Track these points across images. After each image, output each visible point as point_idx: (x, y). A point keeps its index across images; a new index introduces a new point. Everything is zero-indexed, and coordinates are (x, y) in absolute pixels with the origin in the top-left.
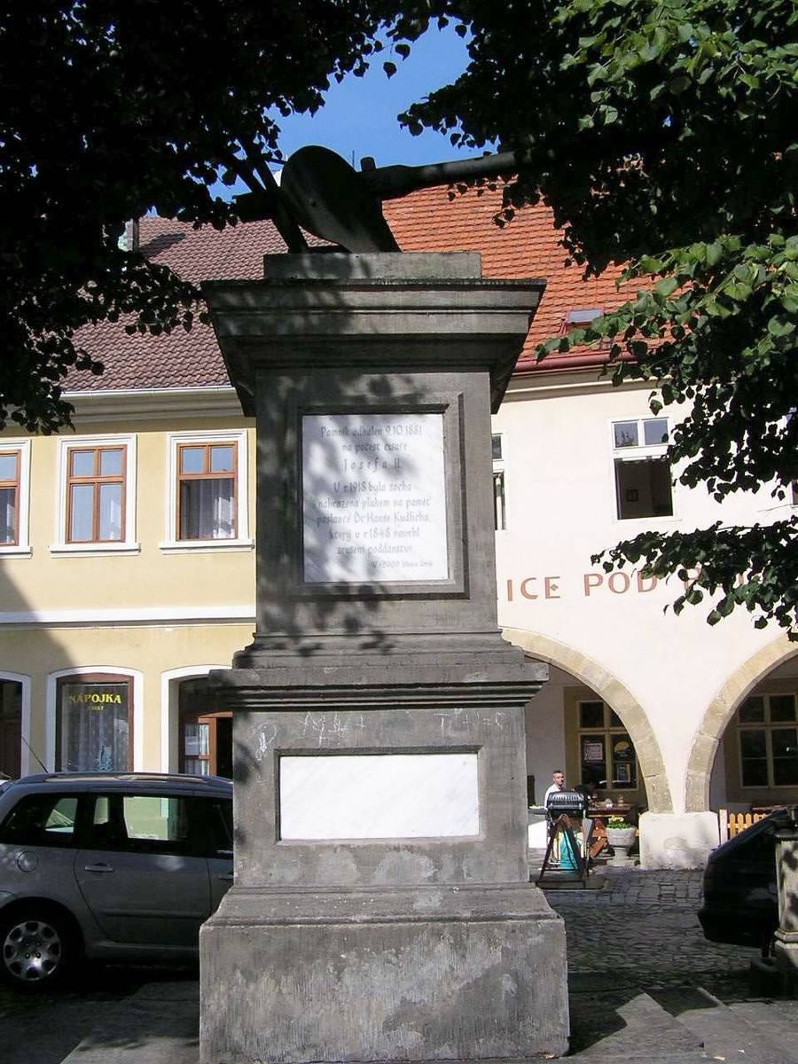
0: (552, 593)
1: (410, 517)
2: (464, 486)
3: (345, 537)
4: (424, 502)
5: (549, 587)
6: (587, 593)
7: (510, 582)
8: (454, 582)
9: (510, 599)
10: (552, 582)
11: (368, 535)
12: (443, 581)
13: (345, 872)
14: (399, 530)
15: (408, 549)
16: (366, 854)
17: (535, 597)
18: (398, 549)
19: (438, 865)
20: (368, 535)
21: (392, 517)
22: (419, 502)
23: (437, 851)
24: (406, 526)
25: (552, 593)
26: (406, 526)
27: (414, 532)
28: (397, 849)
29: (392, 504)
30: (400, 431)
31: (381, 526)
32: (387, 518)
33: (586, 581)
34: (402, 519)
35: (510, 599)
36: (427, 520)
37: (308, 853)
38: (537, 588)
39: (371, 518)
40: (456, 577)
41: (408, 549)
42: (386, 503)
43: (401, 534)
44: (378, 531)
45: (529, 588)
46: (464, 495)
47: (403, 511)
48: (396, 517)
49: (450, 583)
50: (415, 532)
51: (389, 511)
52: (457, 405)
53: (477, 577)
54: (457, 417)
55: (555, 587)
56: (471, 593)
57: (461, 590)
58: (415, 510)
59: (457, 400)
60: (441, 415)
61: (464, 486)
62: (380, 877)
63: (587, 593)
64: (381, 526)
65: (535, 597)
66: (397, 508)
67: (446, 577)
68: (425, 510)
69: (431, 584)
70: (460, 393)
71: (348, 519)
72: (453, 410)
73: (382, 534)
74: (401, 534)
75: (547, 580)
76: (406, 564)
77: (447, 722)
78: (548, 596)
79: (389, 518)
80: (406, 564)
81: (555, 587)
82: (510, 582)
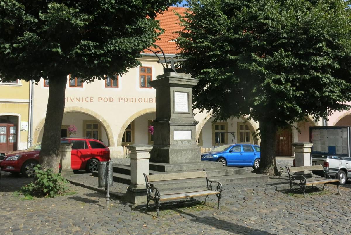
1: (184, 105)
4: (186, 103)
6: (99, 101)
7: (82, 98)
9: (82, 101)
10: (92, 99)
13: (180, 143)
16: (182, 141)
17: (88, 101)
19: (188, 143)
23: (188, 141)
25: (92, 101)
28: (185, 141)
33: (99, 99)
35: (82, 101)
37: (177, 141)
38: (88, 100)
45: (87, 99)
55: (92, 100)
62: (183, 144)
63: (99, 101)
65: (88, 101)
75: (91, 98)
77: (187, 127)
78: (91, 102)
81: (92, 100)
82: (82, 98)
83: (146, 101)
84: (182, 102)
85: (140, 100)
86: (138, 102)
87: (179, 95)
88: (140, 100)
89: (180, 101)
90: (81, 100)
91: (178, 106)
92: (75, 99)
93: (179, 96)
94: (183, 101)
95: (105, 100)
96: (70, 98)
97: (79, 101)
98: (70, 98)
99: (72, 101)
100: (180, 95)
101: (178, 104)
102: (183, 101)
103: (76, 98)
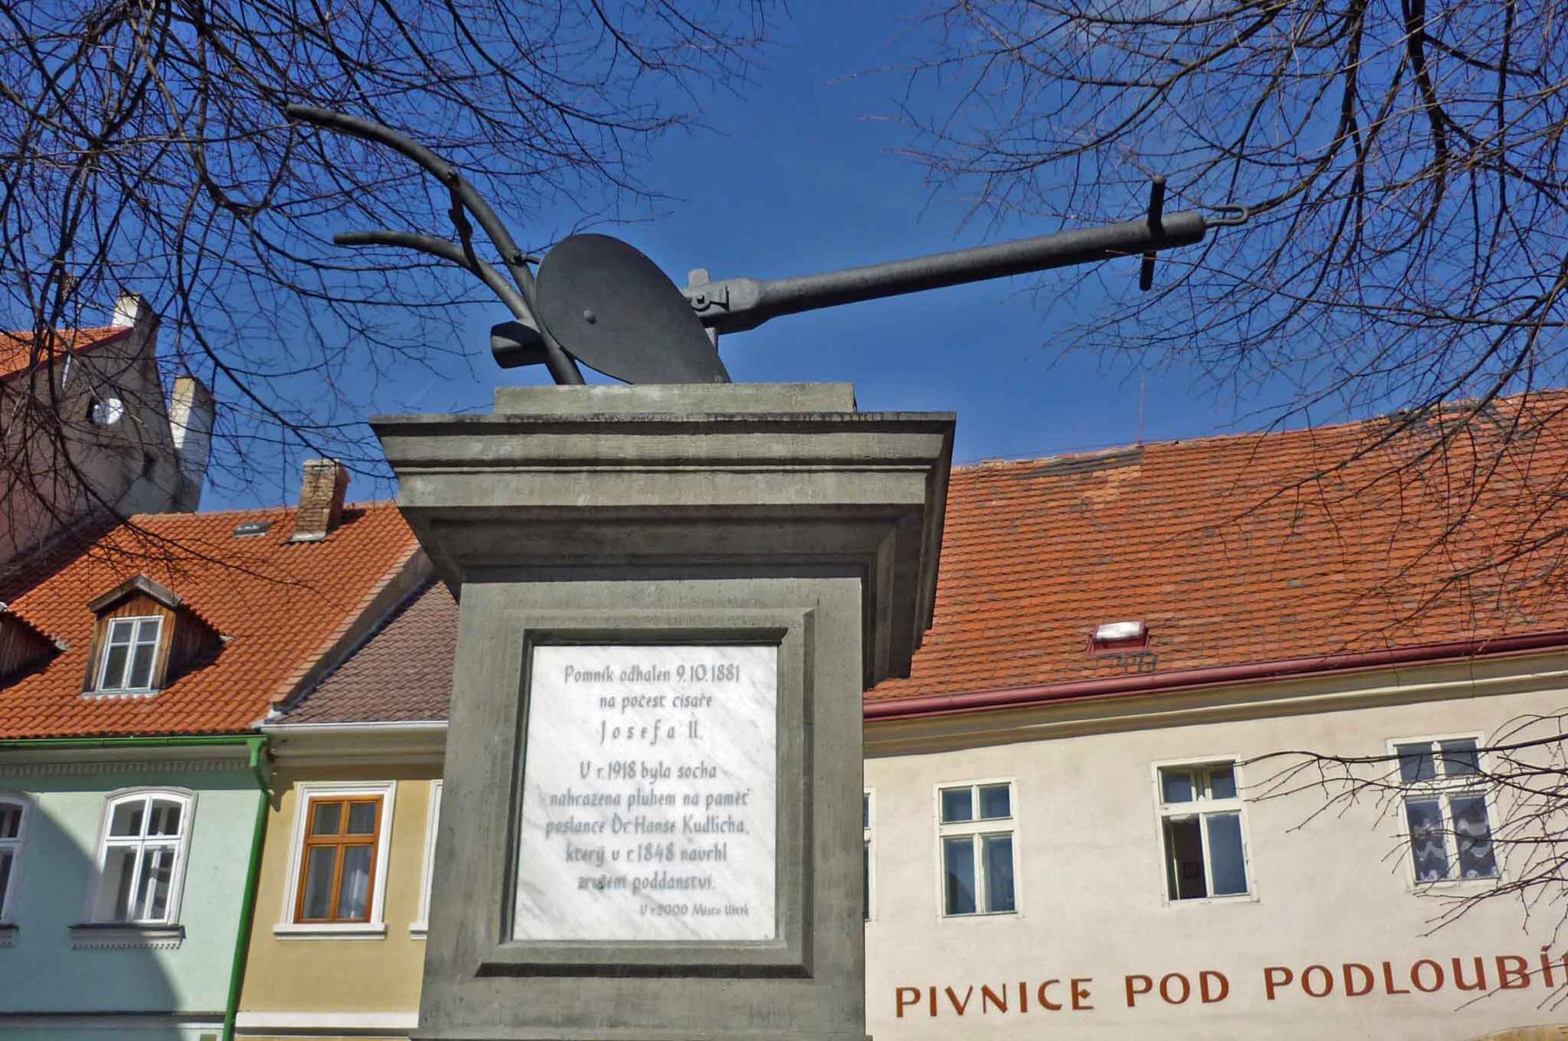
0: (1082, 1002)
1: (710, 826)
2: (809, 771)
3: (594, 857)
5: (1078, 994)
6: (1131, 1003)
7: (1023, 987)
8: (785, 946)
9: (1024, 1009)
10: (1081, 987)
11: (634, 856)
12: (766, 942)
14: (690, 848)
15: (705, 883)
17: (1058, 1007)
18: (683, 884)
20: (634, 856)
21: (679, 825)
22: (728, 799)
24: (706, 841)
25: (1082, 1002)
26: (706, 841)
27: (717, 852)
29: (679, 801)
30: (701, 676)
31: (659, 840)
32: (669, 827)
34: (700, 829)
35: (1024, 1009)
36: (741, 830)
38: (1060, 994)
39: (640, 825)
40: (789, 937)
41: (705, 883)
42: (671, 799)
43: (694, 856)
44: (654, 850)
45: (1052, 995)
46: (809, 788)
47: (699, 814)
48: (686, 825)
49: (779, 946)
50: (719, 854)
51: (676, 813)
52: (802, 630)
53: (829, 936)
54: (801, 652)
55: (1085, 994)
56: (815, 966)
57: (796, 959)
58: (722, 813)
59: (802, 621)
60: (774, 649)
61: (809, 771)
63: (1131, 1003)
64: (659, 840)
65: (1058, 1007)
66: (690, 809)
67: (772, 936)
68: (737, 812)
69: (742, 948)
70: (808, 610)
71: (602, 827)
72: (796, 635)
73: (659, 854)
74: (694, 856)
75: (1075, 983)
76: (700, 910)
78: (1076, 1006)
79: (673, 826)
80: (700, 910)
81: (1085, 994)
82: (1023, 987)
83: (1470, 977)
84: (662, 787)
85: (1428, 976)
86: (1410, 986)
87: (616, 690)
88: (1428, 976)
89: (623, 769)
90: (1014, 1002)
91: (572, 855)
92: (977, 995)
93: (606, 703)
94: (684, 773)
95: (1170, 995)
96: (950, 992)
97: (1003, 1007)
98: (950, 992)
99: (960, 1010)
100: (639, 689)
101: (581, 814)
102: (684, 773)
103: (986, 992)
